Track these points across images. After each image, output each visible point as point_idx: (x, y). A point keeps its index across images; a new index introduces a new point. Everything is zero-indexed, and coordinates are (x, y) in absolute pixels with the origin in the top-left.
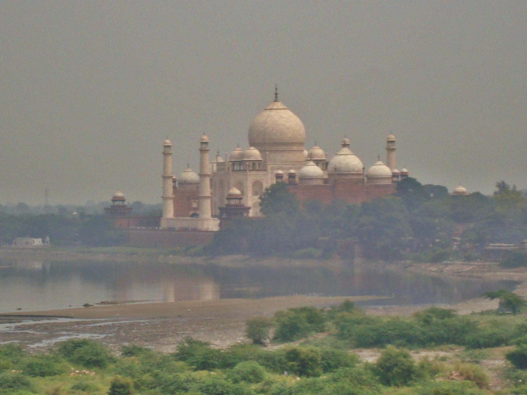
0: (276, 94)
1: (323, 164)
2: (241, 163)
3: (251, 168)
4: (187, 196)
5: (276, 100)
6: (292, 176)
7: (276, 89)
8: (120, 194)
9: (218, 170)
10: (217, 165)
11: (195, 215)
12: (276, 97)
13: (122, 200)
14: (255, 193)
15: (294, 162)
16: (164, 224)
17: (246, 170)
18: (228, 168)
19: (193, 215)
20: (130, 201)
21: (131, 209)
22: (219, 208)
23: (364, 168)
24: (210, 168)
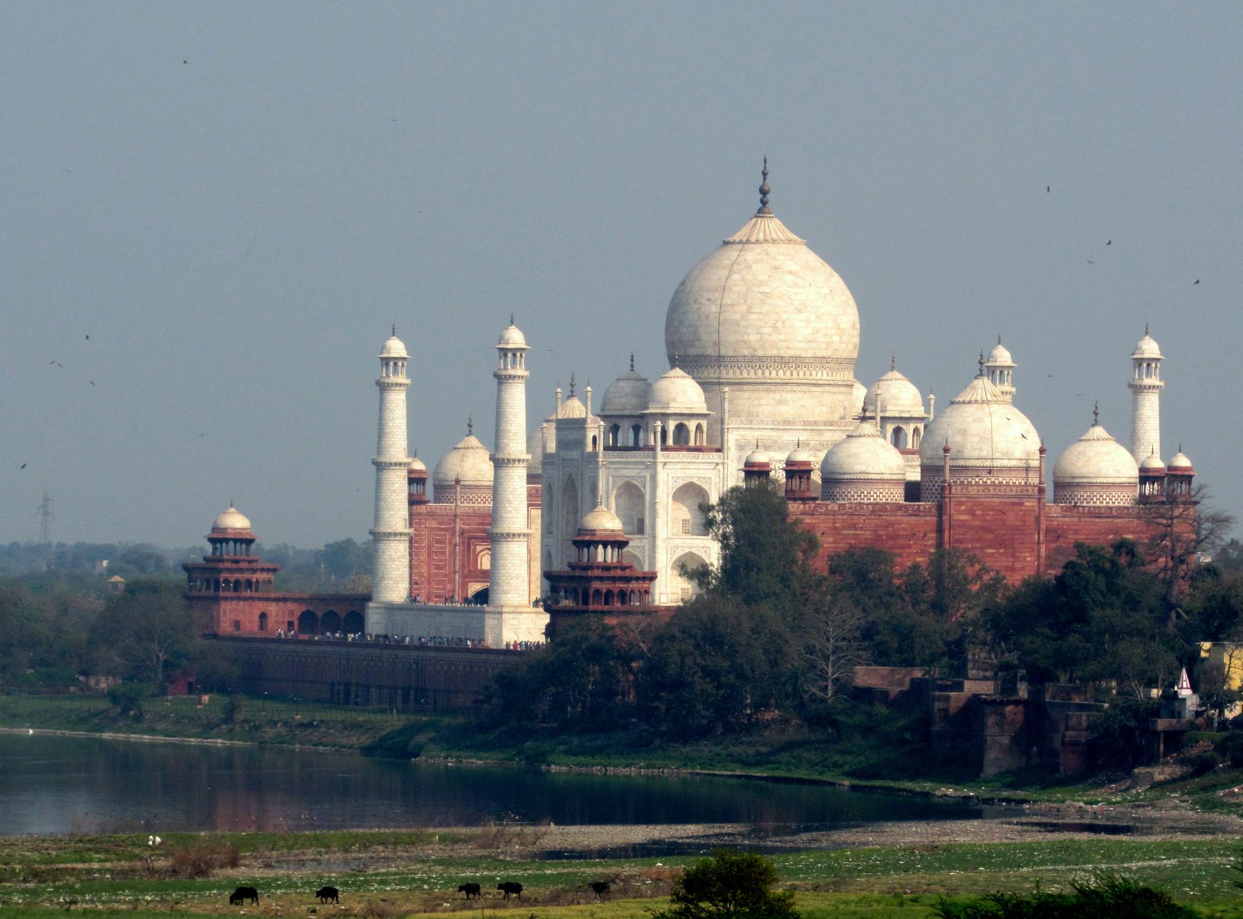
0: (764, 192)
3: (670, 442)
7: (765, 174)
9: (561, 444)
10: (558, 429)
15: (815, 423)
17: (653, 449)
18: (594, 438)
23: (1042, 451)
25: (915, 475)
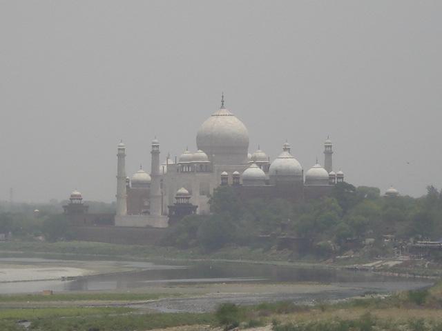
0: (223, 101)
1: (266, 167)
2: (189, 165)
4: (138, 195)
5: (222, 107)
6: (236, 177)
8: (76, 193)
11: (147, 213)
12: (223, 104)
13: (79, 197)
14: (202, 193)
16: (118, 223)
19: (145, 213)
20: (85, 199)
21: (87, 207)
22: (169, 207)
24: (163, 168)
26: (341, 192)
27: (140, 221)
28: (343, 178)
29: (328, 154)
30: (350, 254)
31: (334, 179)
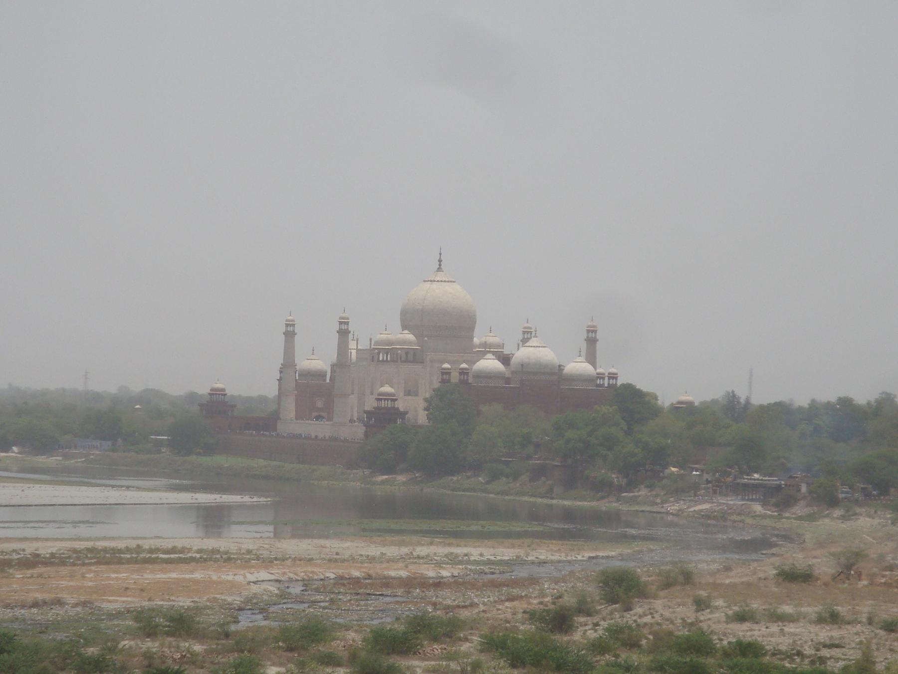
0: (440, 261)
2: (387, 352)
4: (314, 392)
12: (440, 265)
25: (508, 374)
26: (632, 403)
27: (321, 429)
28: (616, 378)
29: (592, 342)
30: (643, 492)
31: (603, 378)
